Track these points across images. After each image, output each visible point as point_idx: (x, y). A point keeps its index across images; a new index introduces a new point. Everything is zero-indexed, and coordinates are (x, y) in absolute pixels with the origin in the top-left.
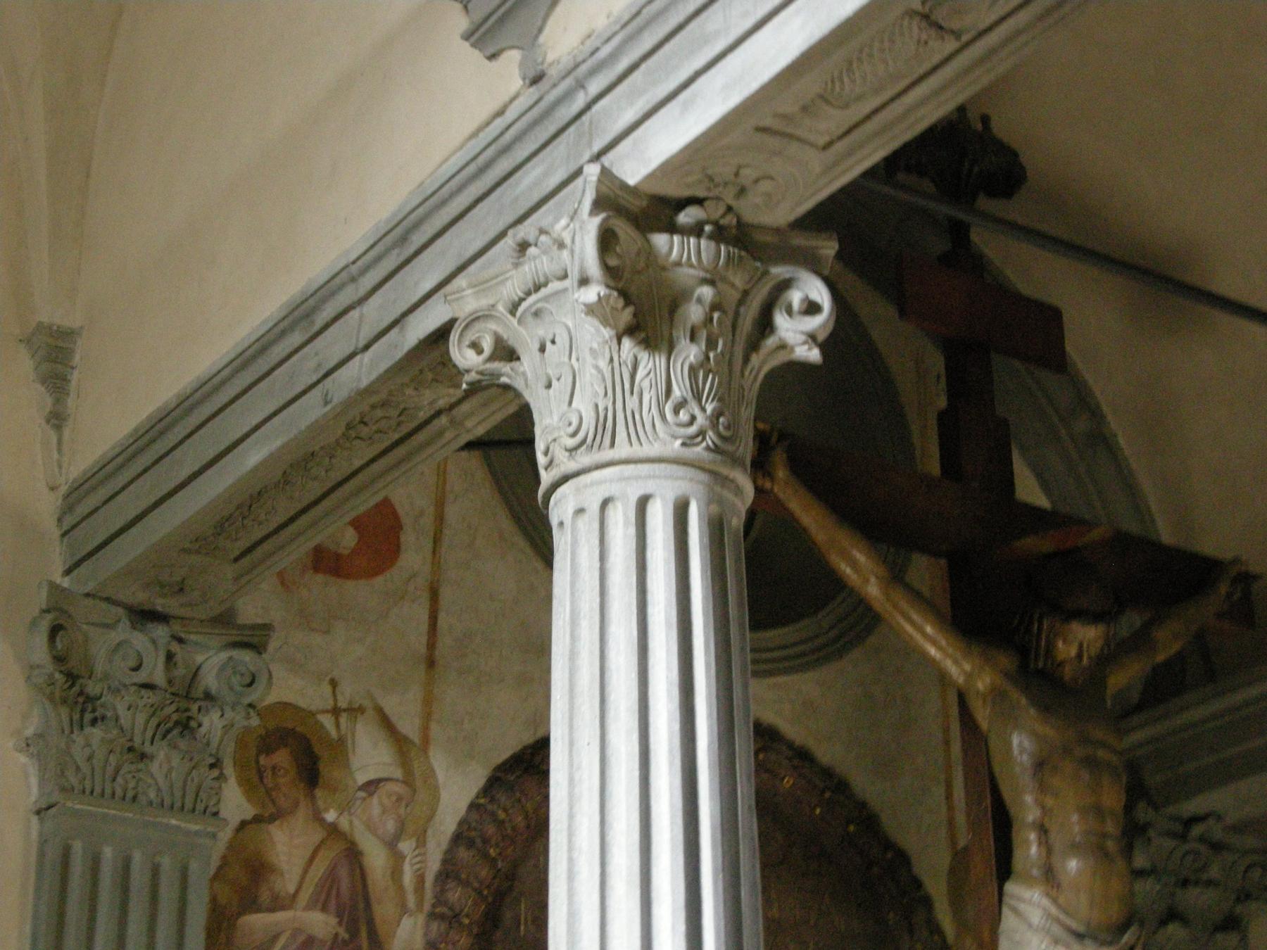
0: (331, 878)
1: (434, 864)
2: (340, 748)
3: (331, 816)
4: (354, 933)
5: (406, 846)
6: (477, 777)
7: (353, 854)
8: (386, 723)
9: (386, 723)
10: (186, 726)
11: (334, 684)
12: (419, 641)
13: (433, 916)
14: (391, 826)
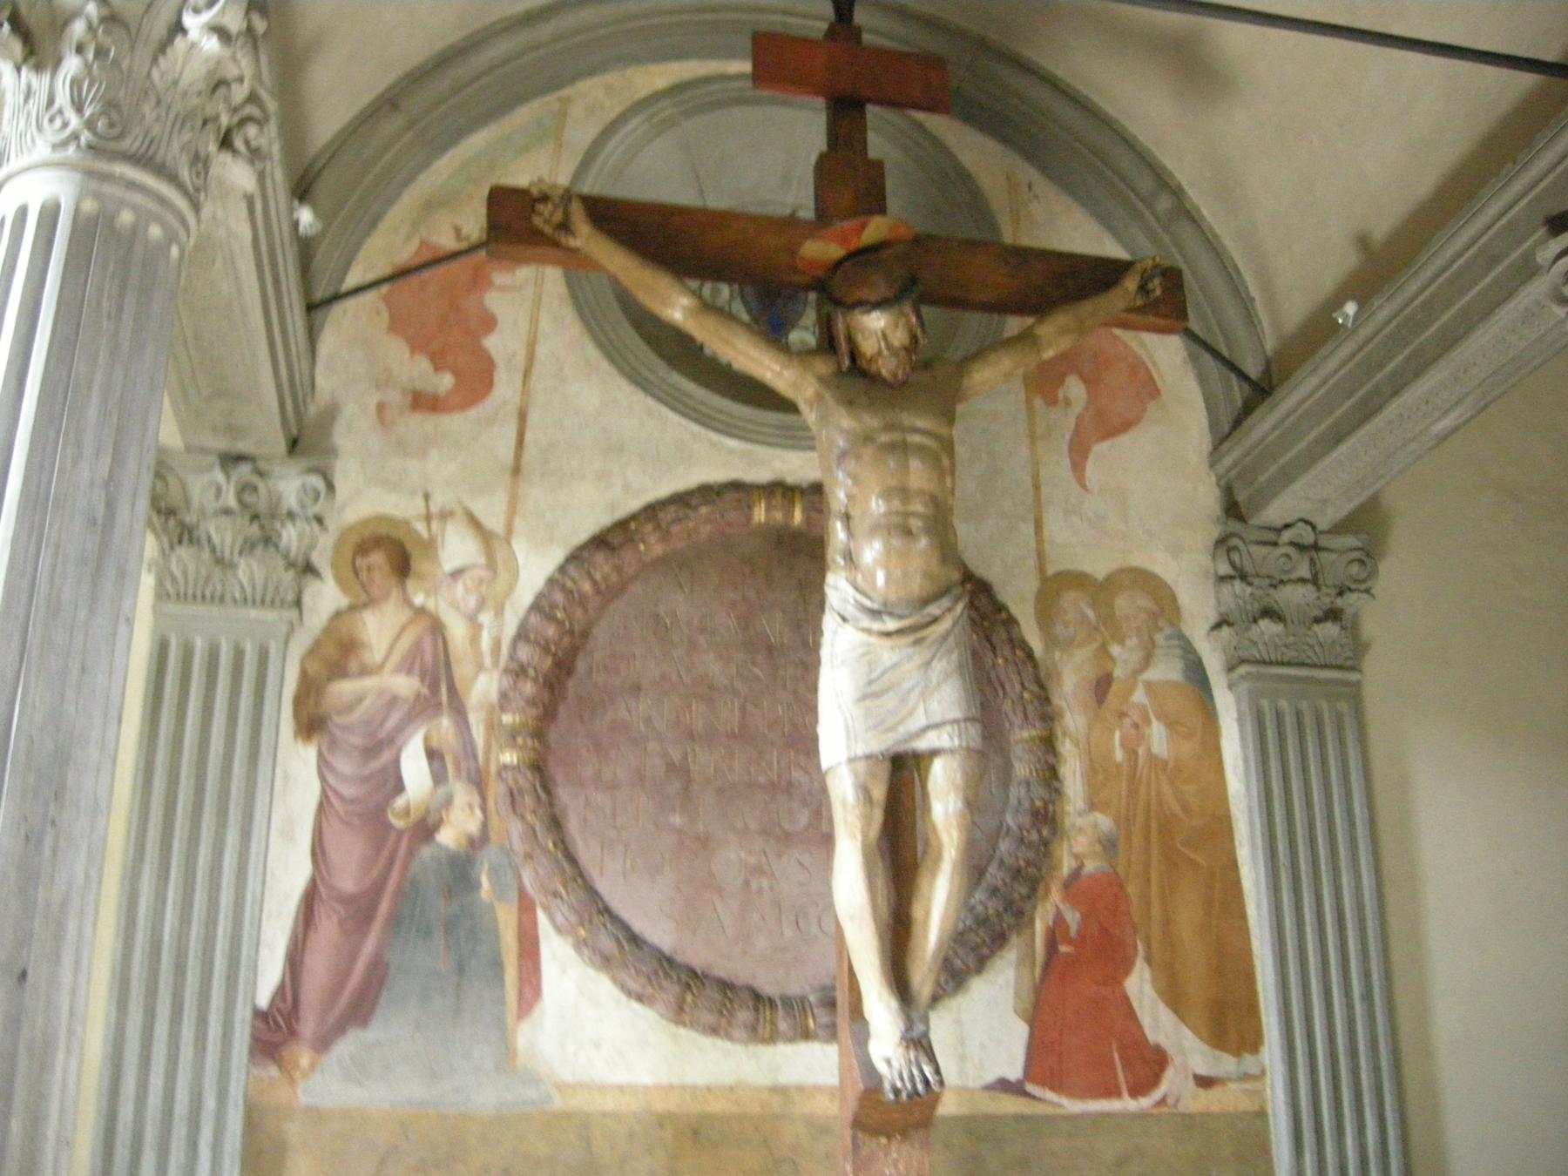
0: (416, 650)
1: (510, 629)
2: (430, 547)
3: (419, 599)
4: (434, 688)
5: (486, 618)
6: (557, 555)
7: (437, 628)
8: (474, 522)
9: (474, 522)
10: (268, 540)
11: (427, 497)
12: (506, 452)
13: (507, 671)
14: (472, 602)
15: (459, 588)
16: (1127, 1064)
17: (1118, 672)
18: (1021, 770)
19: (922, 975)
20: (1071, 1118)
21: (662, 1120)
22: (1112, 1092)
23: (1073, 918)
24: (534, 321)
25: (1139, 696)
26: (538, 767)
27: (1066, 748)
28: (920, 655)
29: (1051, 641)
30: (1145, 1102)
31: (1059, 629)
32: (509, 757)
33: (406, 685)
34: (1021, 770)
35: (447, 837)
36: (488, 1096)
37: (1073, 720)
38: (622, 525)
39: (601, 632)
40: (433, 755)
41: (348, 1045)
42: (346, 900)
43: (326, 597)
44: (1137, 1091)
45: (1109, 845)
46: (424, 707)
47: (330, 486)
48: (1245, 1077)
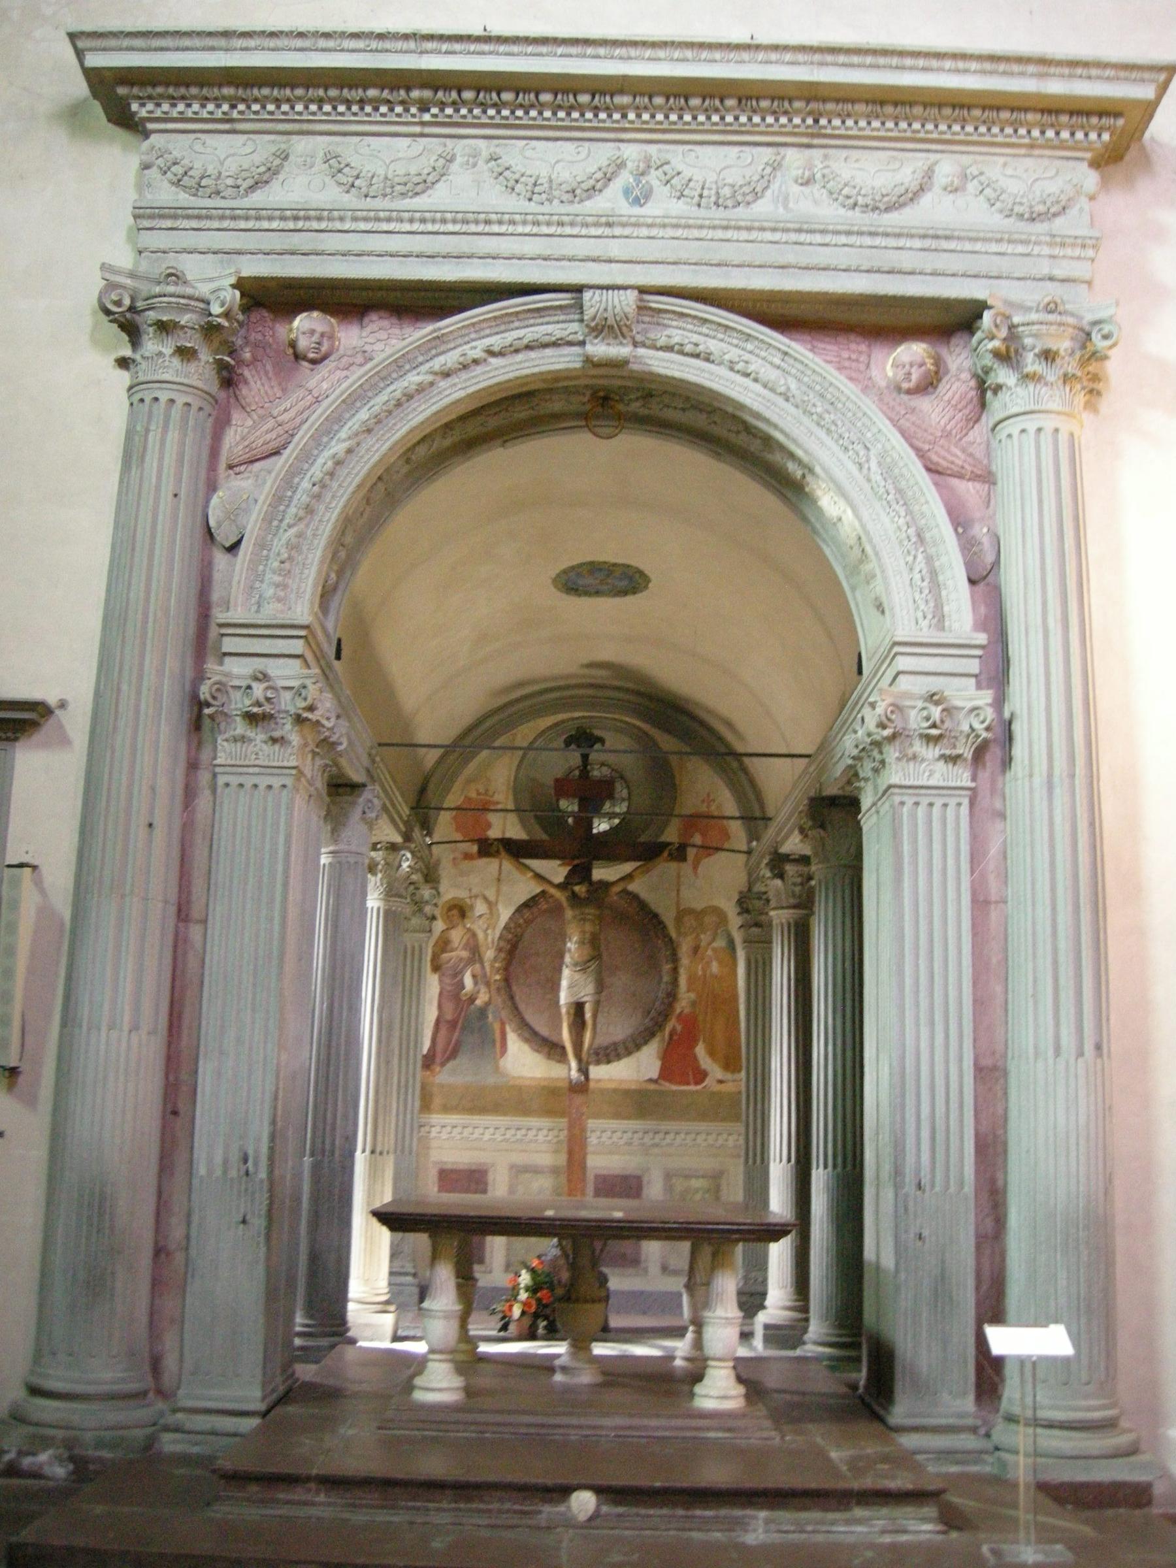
0: (467, 944)
2: (472, 907)
7: (474, 935)
8: (485, 899)
9: (485, 899)
10: (420, 910)
12: (496, 874)
15: (481, 922)
16: (694, 1075)
17: (703, 944)
18: (666, 978)
19: (584, 1055)
20: (674, 1092)
21: (544, 1088)
22: (688, 1084)
23: (679, 1028)
24: (505, 824)
25: (709, 952)
26: (507, 980)
27: (682, 971)
28: (585, 976)
29: (679, 934)
30: (699, 1087)
31: (682, 930)
32: (498, 977)
33: (465, 954)
34: (666, 978)
35: (478, 1002)
36: (491, 1080)
37: (685, 961)
38: (533, 898)
39: (526, 936)
40: (474, 976)
41: (450, 1065)
42: (448, 1022)
43: (439, 926)
44: (697, 1083)
45: (694, 1004)
46: (470, 961)
47: (439, 893)
48: (734, 1081)
